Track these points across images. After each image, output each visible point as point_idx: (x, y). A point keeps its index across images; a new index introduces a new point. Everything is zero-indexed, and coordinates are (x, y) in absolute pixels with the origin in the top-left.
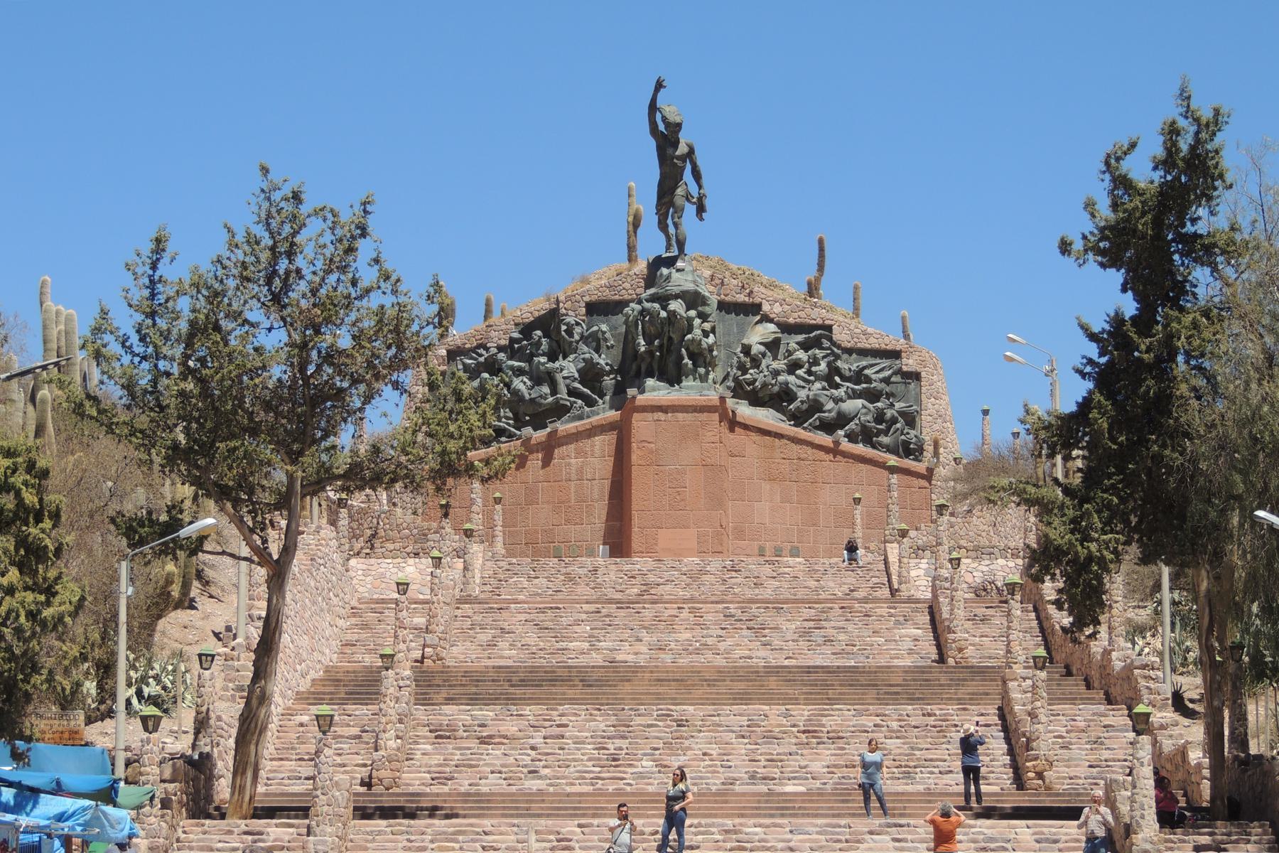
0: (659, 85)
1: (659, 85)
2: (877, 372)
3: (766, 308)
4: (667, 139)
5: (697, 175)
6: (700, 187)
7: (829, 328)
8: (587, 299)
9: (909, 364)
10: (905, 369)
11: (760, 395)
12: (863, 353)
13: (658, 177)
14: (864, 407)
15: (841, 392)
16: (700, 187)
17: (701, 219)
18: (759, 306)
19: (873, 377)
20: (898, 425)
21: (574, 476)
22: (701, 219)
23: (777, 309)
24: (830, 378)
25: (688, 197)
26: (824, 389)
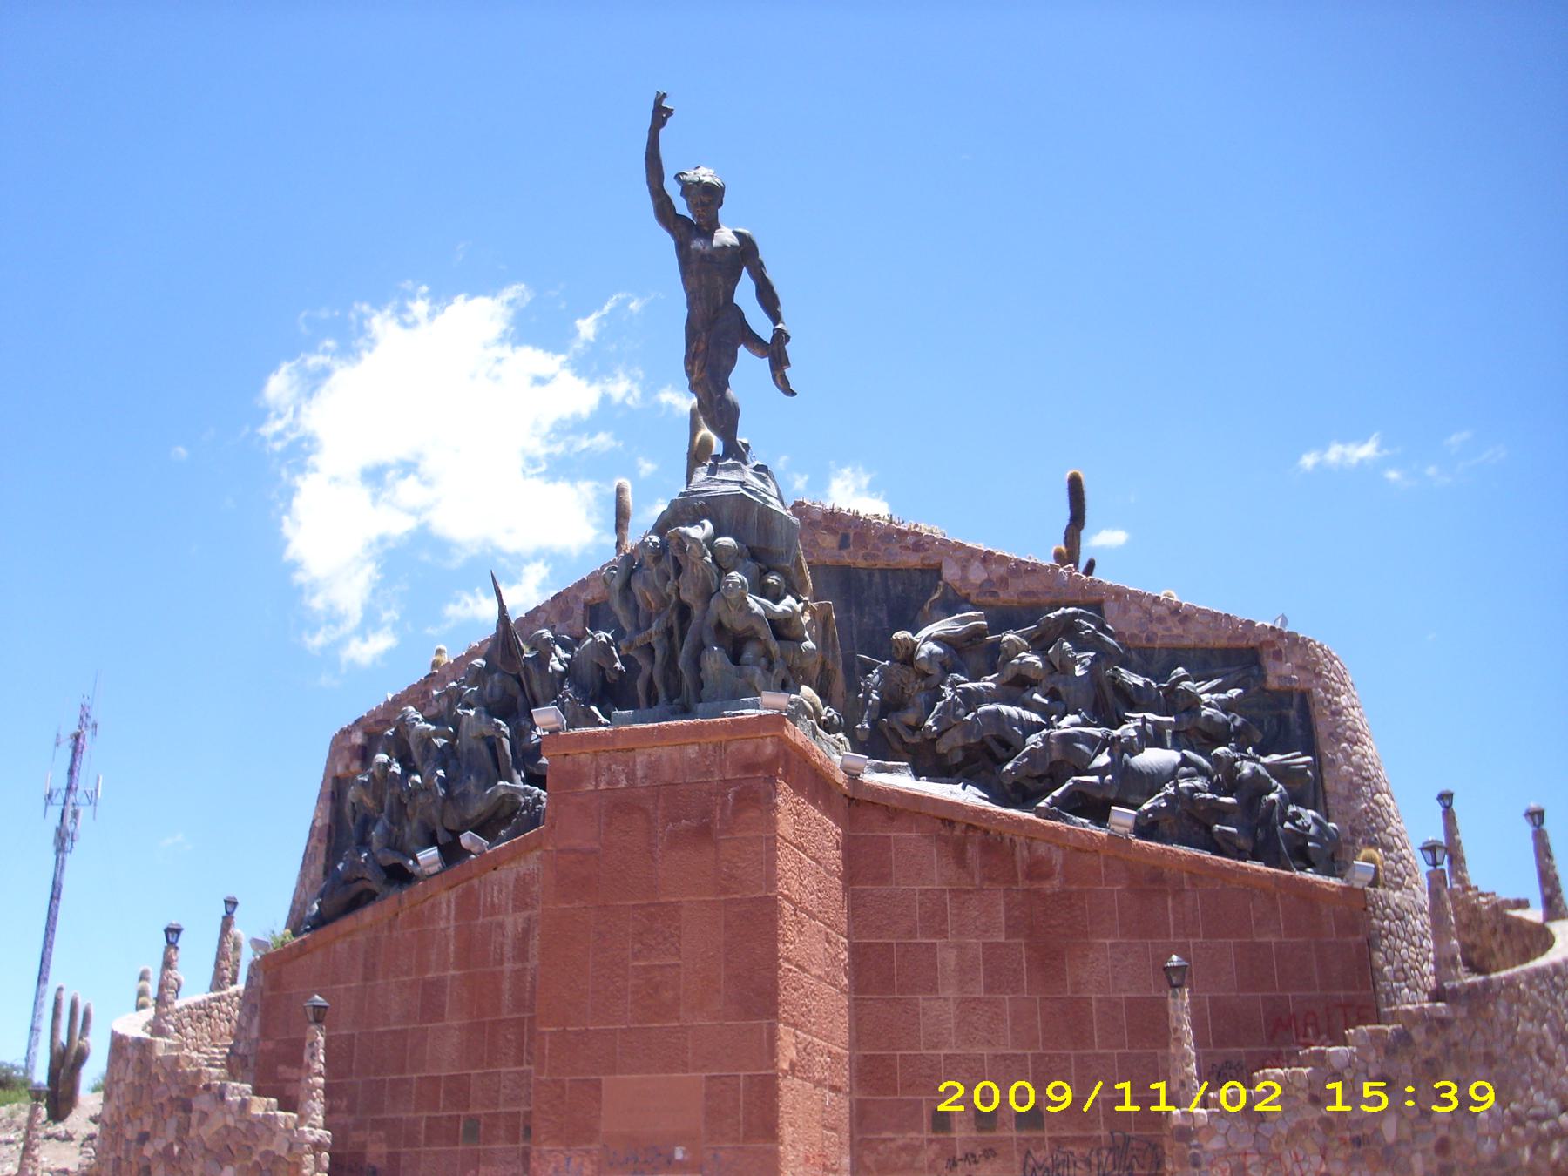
0: (660, 115)
1: (660, 115)
2: (1207, 691)
3: (950, 573)
4: (690, 217)
5: (768, 298)
6: (776, 317)
7: (1097, 607)
8: (586, 596)
9: (1280, 673)
10: (1273, 683)
11: (942, 748)
12: (1176, 656)
13: (686, 311)
14: (1186, 761)
15: (1128, 730)
16: (776, 317)
17: (793, 394)
18: (937, 571)
19: (1206, 698)
20: (1273, 796)
21: (508, 951)
22: (793, 394)
23: (977, 574)
24: (1108, 704)
25: (753, 341)
26: (1085, 723)
